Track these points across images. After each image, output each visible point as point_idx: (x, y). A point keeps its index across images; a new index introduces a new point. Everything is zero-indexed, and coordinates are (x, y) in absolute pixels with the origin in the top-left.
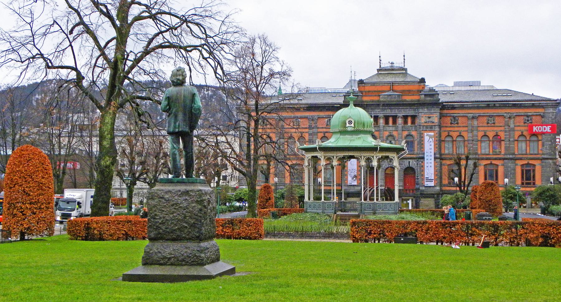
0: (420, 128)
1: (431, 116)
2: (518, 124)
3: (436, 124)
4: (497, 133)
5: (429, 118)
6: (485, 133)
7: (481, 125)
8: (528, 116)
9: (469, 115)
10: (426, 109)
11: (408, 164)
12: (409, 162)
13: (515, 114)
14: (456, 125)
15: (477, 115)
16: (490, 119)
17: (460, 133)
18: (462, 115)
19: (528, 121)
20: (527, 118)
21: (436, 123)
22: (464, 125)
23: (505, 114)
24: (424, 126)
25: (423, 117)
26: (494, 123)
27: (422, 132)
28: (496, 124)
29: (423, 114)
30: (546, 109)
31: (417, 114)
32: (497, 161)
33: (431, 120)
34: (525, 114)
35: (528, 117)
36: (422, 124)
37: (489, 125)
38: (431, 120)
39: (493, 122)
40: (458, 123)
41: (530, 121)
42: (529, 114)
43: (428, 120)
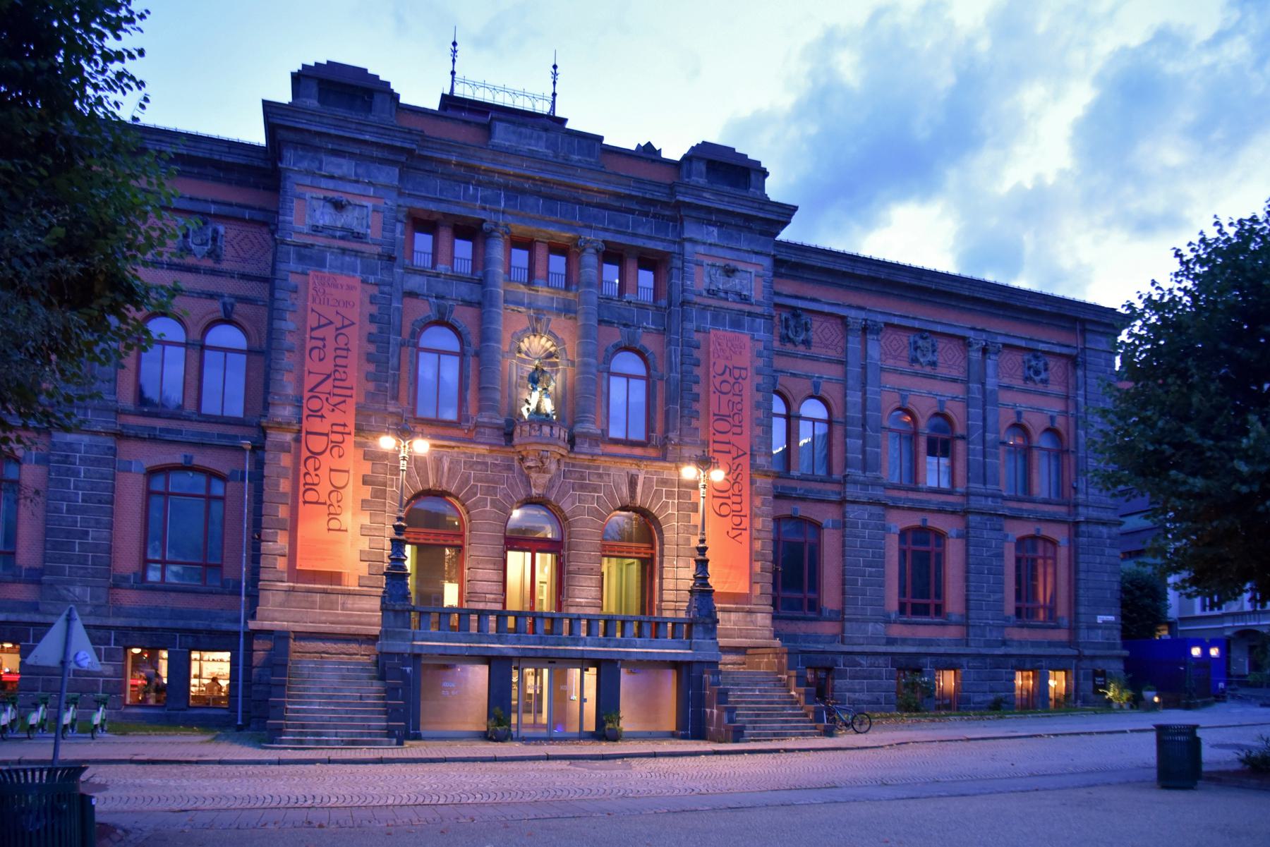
0: (685, 318)
1: (741, 266)
2: (1006, 381)
3: (759, 310)
4: (941, 403)
5: (730, 272)
6: (904, 398)
7: (890, 363)
8: (1035, 353)
9: (852, 314)
10: (715, 230)
11: (625, 490)
12: (633, 483)
13: (1000, 339)
14: (801, 349)
15: (880, 319)
16: (920, 343)
17: (816, 386)
18: (827, 309)
19: (1037, 373)
20: (1033, 363)
21: (758, 304)
22: (832, 354)
23: (971, 334)
24: (706, 307)
25: (699, 264)
26: (933, 364)
27: (697, 337)
28: (942, 371)
29: (701, 249)
30: (1089, 336)
31: (675, 248)
32: (941, 517)
33: (735, 283)
34: (1031, 345)
35: (1036, 358)
36: (696, 299)
37: (917, 367)
38: (735, 283)
39: (930, 357)
40: (806, 343)
41: (1043, 376)
42: (1041, 347)
43: (722, 283)
